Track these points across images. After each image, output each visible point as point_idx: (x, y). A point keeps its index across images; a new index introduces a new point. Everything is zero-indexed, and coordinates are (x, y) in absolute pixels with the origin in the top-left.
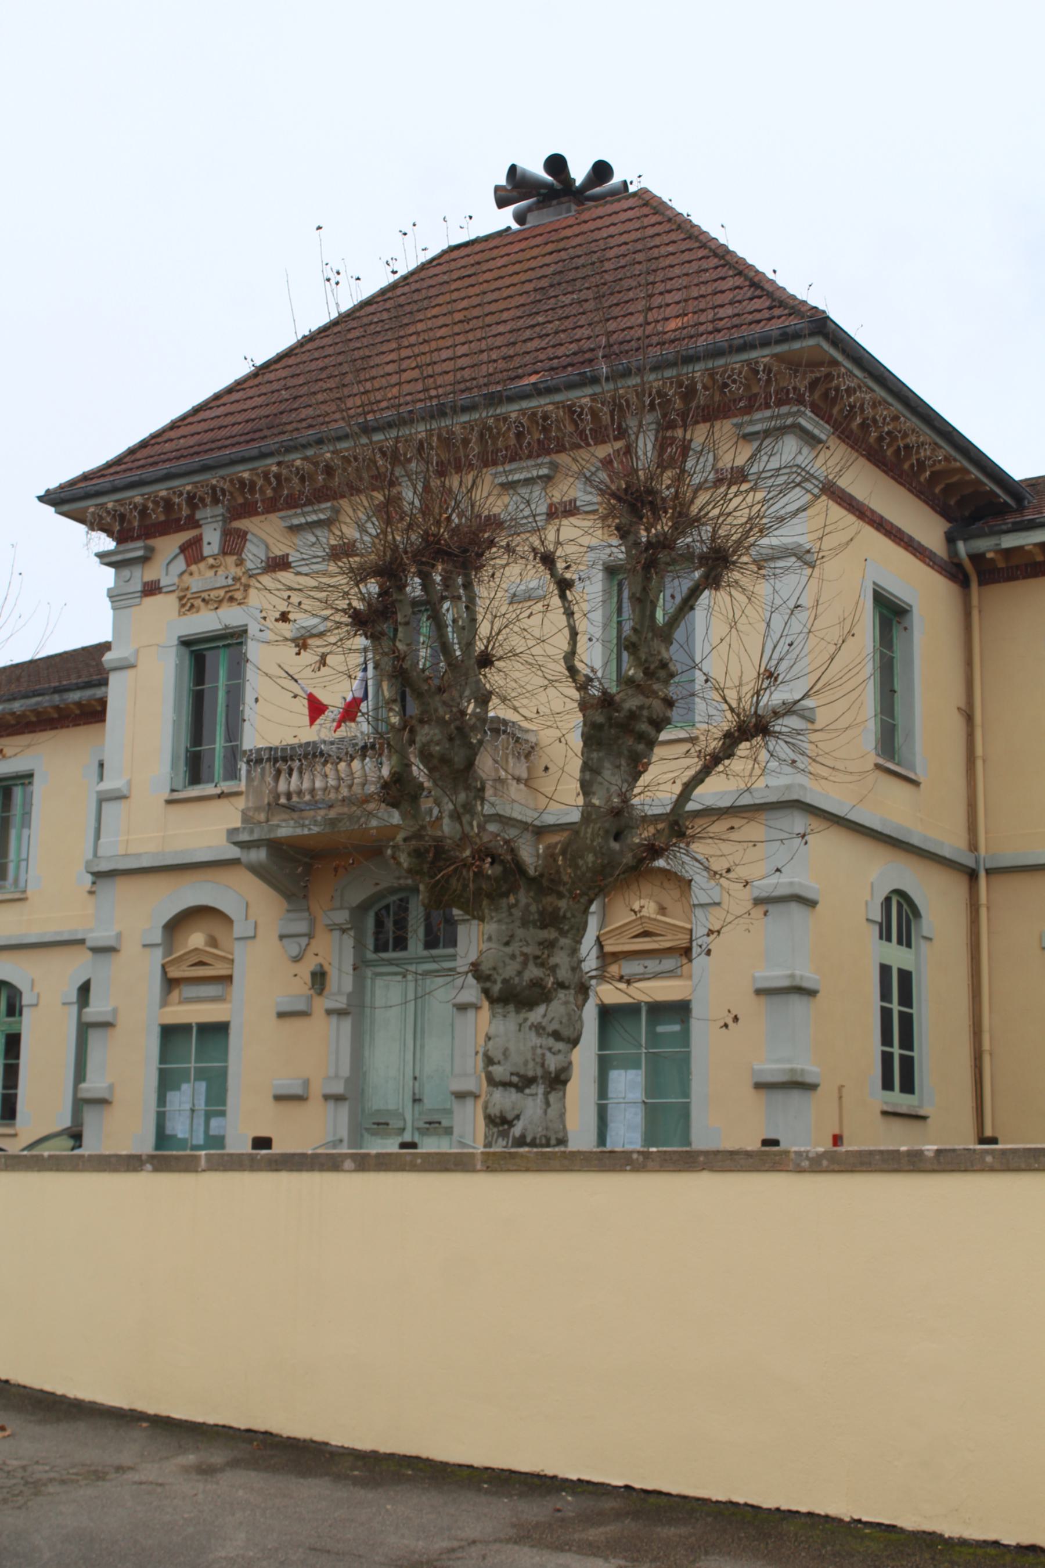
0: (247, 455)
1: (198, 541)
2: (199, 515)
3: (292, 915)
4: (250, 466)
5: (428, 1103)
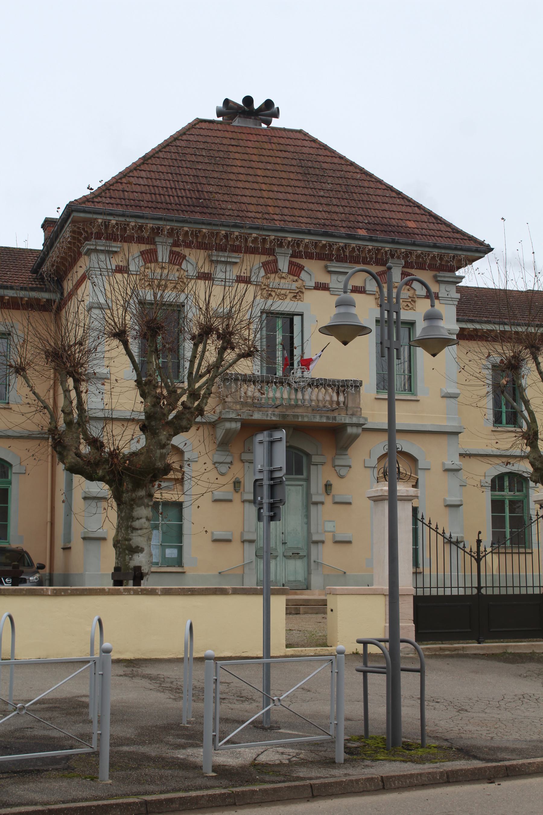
0: (214, 223)
1: (154, 252)
2: (157, 239)
3: (219, 452)
4: (209, 227)
5: (289, 545)
